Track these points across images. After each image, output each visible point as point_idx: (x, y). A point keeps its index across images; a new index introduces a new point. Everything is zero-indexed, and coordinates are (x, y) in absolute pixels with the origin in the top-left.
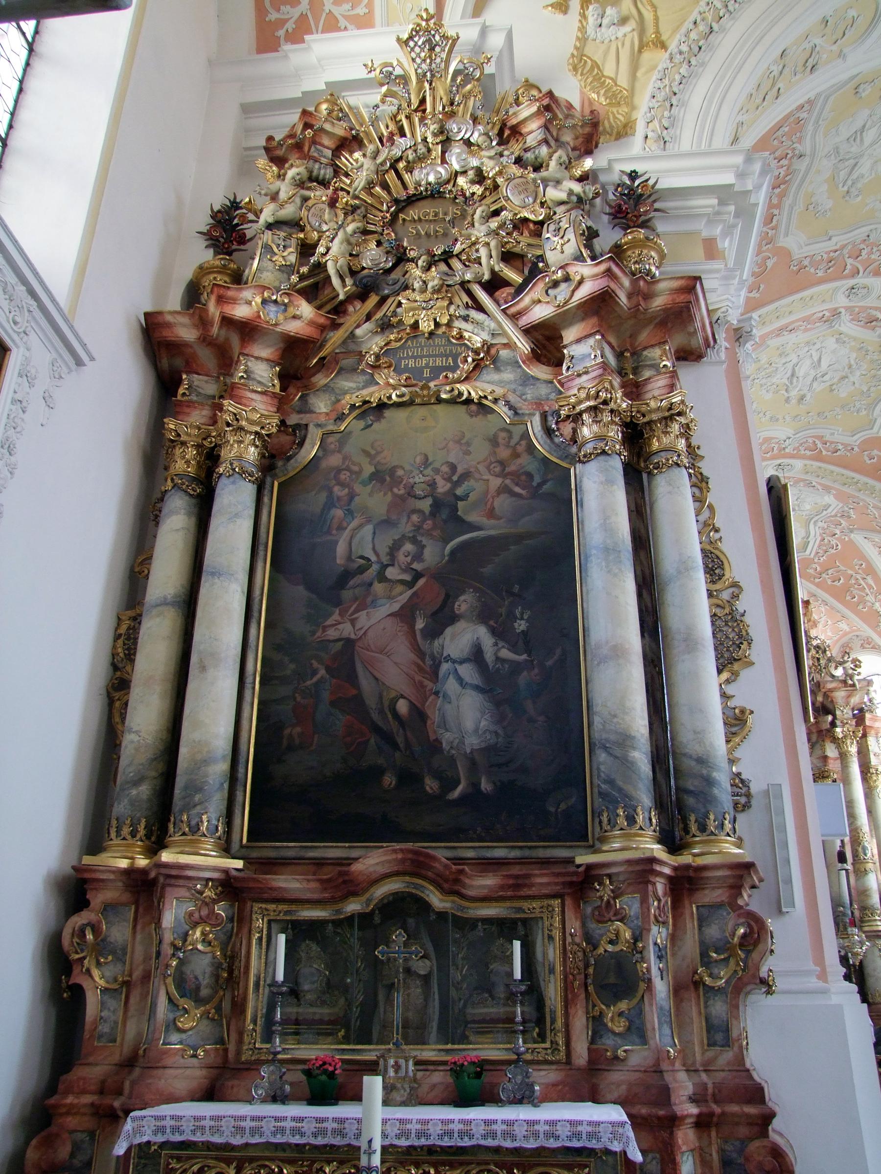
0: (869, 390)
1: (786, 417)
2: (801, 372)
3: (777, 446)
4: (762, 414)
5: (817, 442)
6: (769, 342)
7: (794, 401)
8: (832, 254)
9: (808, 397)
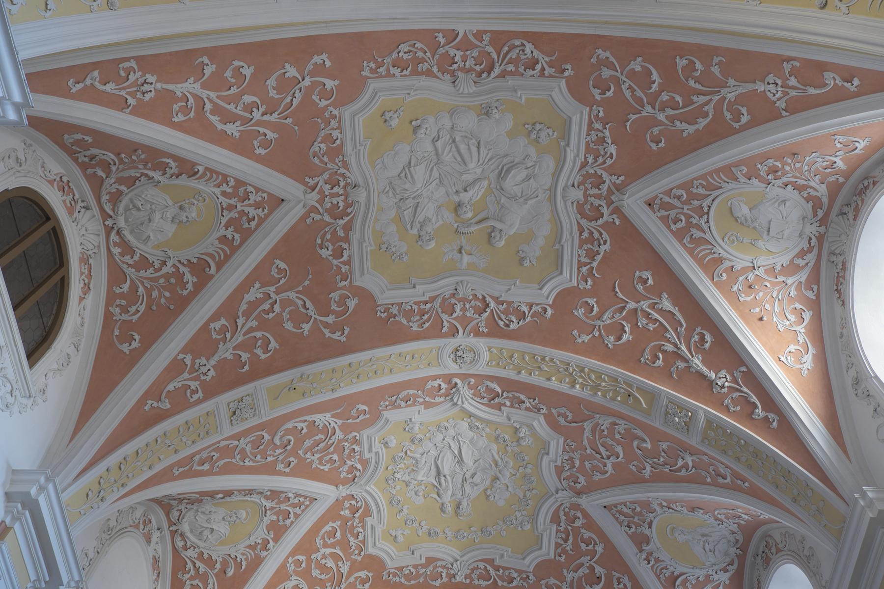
0: (525, 496)
1: (447, 531)
2: (446, 470)
3: (445, 571)
4: (416, 525)
5: (489, 568)
6: (386, 414)
7: (450, 509)
8: (422, 306)
9: (464, 504)
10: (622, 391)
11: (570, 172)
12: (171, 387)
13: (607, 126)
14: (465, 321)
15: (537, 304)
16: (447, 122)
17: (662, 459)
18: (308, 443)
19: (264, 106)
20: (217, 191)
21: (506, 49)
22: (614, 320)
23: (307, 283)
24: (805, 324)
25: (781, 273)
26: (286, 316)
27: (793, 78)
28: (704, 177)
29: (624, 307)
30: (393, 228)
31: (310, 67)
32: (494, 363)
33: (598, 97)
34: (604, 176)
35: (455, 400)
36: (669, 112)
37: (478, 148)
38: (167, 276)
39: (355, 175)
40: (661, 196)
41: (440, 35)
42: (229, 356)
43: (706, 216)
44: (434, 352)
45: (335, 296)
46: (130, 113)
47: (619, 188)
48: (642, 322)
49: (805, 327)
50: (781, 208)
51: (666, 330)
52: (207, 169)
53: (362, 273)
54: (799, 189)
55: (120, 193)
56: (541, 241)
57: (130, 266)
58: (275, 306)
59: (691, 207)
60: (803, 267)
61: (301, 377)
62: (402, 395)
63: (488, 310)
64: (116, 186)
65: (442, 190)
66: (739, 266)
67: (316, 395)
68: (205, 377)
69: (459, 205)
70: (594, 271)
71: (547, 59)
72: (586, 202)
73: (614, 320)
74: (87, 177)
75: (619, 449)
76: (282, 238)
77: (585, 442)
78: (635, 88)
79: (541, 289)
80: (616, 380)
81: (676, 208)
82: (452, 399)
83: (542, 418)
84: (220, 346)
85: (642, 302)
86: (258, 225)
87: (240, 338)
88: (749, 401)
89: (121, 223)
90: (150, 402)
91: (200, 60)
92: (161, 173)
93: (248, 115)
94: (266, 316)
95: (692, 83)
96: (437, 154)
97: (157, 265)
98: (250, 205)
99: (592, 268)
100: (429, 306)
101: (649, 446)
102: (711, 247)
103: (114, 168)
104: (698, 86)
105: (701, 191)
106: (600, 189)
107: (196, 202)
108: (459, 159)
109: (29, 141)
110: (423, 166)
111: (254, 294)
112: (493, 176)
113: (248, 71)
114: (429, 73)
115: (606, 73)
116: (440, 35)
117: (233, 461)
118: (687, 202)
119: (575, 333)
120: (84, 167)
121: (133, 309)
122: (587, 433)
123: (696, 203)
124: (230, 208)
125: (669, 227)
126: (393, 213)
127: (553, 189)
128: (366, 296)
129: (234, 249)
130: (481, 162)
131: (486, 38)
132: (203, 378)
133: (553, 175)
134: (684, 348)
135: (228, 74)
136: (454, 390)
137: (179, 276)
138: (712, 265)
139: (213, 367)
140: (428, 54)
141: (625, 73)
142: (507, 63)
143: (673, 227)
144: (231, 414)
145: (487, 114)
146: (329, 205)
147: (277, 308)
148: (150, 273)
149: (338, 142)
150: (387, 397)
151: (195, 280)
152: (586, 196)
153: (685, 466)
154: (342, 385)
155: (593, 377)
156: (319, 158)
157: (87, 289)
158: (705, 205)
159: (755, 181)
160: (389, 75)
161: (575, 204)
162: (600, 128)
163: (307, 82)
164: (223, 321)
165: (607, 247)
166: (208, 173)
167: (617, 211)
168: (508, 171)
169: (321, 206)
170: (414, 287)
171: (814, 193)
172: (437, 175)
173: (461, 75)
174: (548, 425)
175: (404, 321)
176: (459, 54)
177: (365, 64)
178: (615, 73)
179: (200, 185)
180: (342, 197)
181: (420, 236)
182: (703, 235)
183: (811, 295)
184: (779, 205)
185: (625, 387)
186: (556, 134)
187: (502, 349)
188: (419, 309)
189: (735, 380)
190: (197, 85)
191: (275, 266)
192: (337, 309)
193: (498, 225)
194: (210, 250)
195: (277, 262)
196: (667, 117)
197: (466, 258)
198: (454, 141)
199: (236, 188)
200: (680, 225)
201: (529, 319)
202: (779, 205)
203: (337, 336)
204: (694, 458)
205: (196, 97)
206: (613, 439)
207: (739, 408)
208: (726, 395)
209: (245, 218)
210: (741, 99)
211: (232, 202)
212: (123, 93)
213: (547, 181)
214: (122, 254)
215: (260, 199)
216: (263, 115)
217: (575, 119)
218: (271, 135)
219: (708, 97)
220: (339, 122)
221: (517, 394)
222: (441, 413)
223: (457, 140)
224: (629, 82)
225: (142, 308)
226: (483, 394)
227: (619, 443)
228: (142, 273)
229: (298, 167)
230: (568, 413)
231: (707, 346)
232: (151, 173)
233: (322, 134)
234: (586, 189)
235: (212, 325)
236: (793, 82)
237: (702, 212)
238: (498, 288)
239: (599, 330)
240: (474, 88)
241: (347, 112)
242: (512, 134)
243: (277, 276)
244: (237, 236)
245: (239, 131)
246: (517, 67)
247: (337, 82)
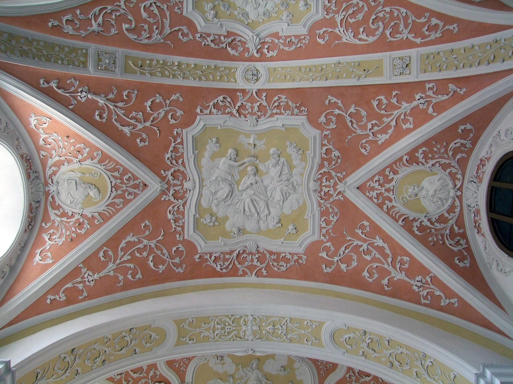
10: (146, 69)
11: (192, 198)
12: (445, 97)
13: (174, 229)
14: (252, 100)
15: (206, 114)
16: (263, 226)
17: (114, 17)
18: (360, 17)
19: (360, 250)
20: (394, 203)
21: (230, 267)
22: (157, 113)
23: (349, 137)
24: (42, 139)
25: (64, 161)
26: (365, 120)
27: (81, 288)
28: (118, 211)
29: (152, 121)
30: (295, 162)
31: (333, 267)
32: (232, 71)
33: (180, 245)
34: (173, 199)
35: (258, 39)
36: (141, 246)
37: (244, 210)
38: (432, 158)
39: (315, 197)
40: (139, 192)
41: (264, 274)
42: (405, 105)
43: (113, 185)
44: (272, 79)
45: (333, 126)
46: (431, 272)
47: (163, 192)
48: (140, 115)
49: (41, 137)
50: (72, 199)
51: (124, 115)
52: (397, 221)
53: (315, 138)
54: (64, 214)
55: (448, 212)
56: (207, 154)
57: (454, 167)
58: (370, 127)
59: (122, 189)
60: (52, 166)
61: (359, 78)
62: (294, 47)
63: (237, 108)
64: (450, 217)
65: (265, 183)
66: (89, 161)
67: (351, 62)
68: (422, 95)
69: (255, 174)
70: (173, 140)
71: (209, 263)
72: (182, 180)
73: (157, 113)
74: (464, 228)
75: (144, 15)
76: (360, 167)
77: (168, 14)
78: (161, 256)
79: (205, 125)
80: (151, 74)
81: (129, 187)
82: (260, 40)
83: (199, 29)
84: (409, 112)
85: (141, 127)
86: (374, 176)
87: (396, 113)
88: (62, 88)
89: (452, 193)
90: (462, 93)
91: (389, 289)
92: (423, 223)
93: (369, 247)
94: (377, 122)
95: (132, 266)
96: (268, 206)
97: (438, 165)
98: (377, 189)
99: (174, 142)
100: (274, 111)
101: (125, 26)
102: (106, 168)
103: (448, 232)
104: (128, 265)
105: (117, 201)
106: (174, 190)
107: (407, 197)
108: (255, 203)
109: (489, 266)
110: (276, 200)
111: (382, 138)
112: (236, 192)
113: (366, 274)
114: (271, 253)
115: (177, 260)
116: (264, 274)
117: (414, 18)
118: (124, 191)
119: (181, 99)
120: (464, 236)
121: (457, 145)
122: (167, 22)
123: (119, 192)
124: (388, 190)
125: (132, 174)
126: (294, 171)
127: (201, 187)
128: (314, 122)
129: (390, 166)
130: (243, 202)
131: (241, 272)
132: (423, 95)
133: (202, 196)
134: (112, 107)
135: (376, 276)
136: (259, 47)
137: (426, 158)
138: (104, 158)
139: (415, 100)
140: (271, 264)
141: (167, 262)
142: (229, 258)
143: (130, 175)
144: (409, 66)
145: (239, 230)
146: (332, 181)
147: (369, 126)
148: (443, 161)
149: (323, 220)
150: (304, 46)
151: (417, 154)
152: (182, 185)
153: (96, 17)
154: (333, 66)
155: (167, 72)
156: (334, 211)
157: (482, 163)
158: (114, 192)
159: (90, 216)
160: (292, 254)
161: (188, 179)
162: (177, 228)
163: (336, 259)
164: (404, 127)
165: (168, 156)
166: (397, 218)
167: (163, 178)
168: (227, 196)
169: (336, 181)
170: (283, 125)
171: (56, 212)
172: (268, 193)
173: (254, 251)
174: (194, 23)
175: (290, 103)
176: (255, 263)
177: (304, 262)
178: (172, 261)
179: (404, 210)
180: (323, 184)
181: (279, 156)
182: (112, 174)
183: (43, 153)
184: (74, 201)
185: (145, 71)
186: (202, 221)
187: (228, 82)
188: (281, 110)
189: (75, 98)
190: (393, 275)
191: (367, 152)
192: (332, 117)
193: (232, 163)
194: (404, 168)
195: (366, 153)
196: (143, 242)
197: (251, 141)
198: (258, 213)
199: (383, 203)
200: (126, 177)
201: (211, 104)
202: (74, 201)
203: (334, 100)
204: (92, 29)
205: (394, 267)
206: (148, 23)
207: (68, 82)
208: (79, 86)
209: (381, 182)
210: (104, 265)
211: (386, 194)
212: (432, 286)
213: (205, 191)
214: (456, 173)
215: (371, 192)
216: (362, 245)
217: (191, 231)
218: (359, 232)
219: (122, 260)
220: (321, 231)
221: (217, 47)
222: (267, 29)
223: (256, 215)
224: (165, 258)
225: (452, 145)
226: (239, 44)
227: (145, 21)
228: (447, 162)
229: (346, 207)
230: (181, 37)
231: (97, 113)
232: (428, 224)
233: (331, 226)
234: (182, 189)
235: (412, 126)
236: (80, 286)
237: (115, 187)
238: (231, 122)
239: (166, 104)
240: (247, 244)
241: (316, 238)
242: (226, 218)
243: (367, 145)
244: (387, 173)
245: (376, 239)
246: (224, 257)
247: (320, 255)
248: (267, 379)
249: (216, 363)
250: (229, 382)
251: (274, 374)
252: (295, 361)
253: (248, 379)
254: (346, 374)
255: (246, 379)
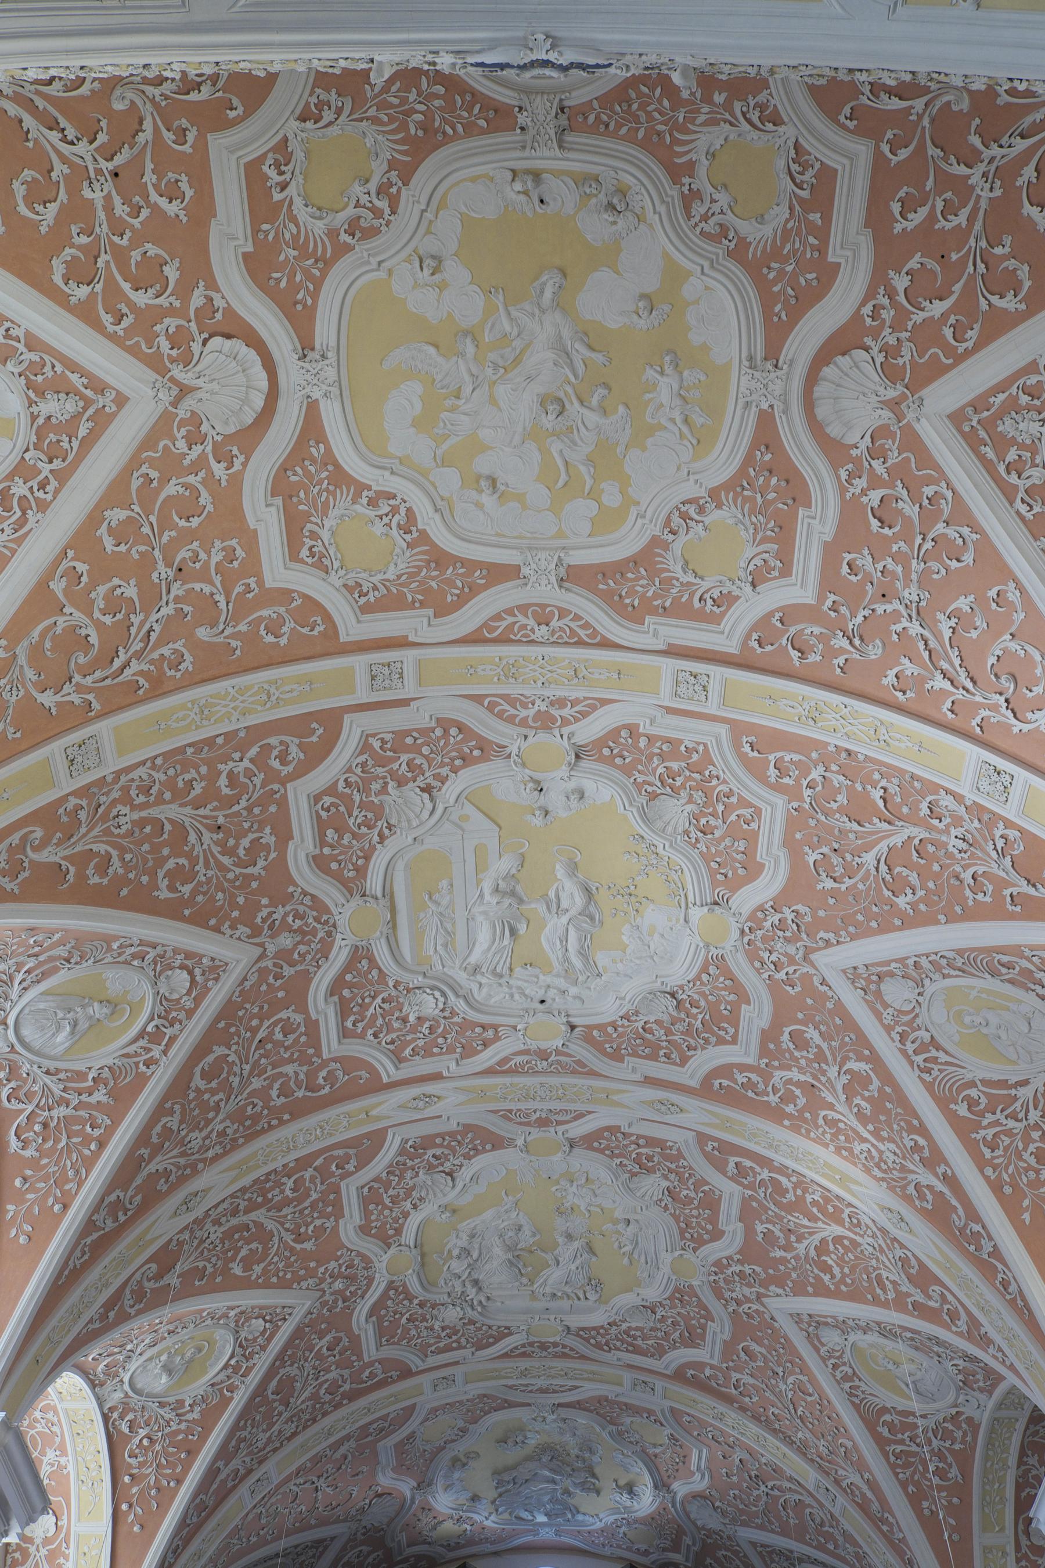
248: (591, 348)
249: (416, 285)
250: (462, 355)
251: (613, 326)
252: (689, 274)
253: (528, 345)
254: (863, 304)
255: (518, 344)
